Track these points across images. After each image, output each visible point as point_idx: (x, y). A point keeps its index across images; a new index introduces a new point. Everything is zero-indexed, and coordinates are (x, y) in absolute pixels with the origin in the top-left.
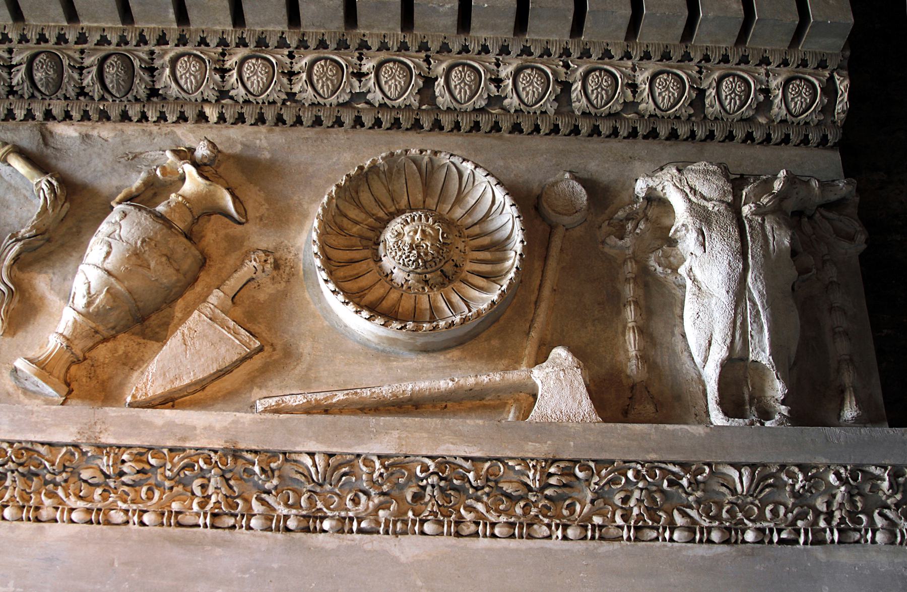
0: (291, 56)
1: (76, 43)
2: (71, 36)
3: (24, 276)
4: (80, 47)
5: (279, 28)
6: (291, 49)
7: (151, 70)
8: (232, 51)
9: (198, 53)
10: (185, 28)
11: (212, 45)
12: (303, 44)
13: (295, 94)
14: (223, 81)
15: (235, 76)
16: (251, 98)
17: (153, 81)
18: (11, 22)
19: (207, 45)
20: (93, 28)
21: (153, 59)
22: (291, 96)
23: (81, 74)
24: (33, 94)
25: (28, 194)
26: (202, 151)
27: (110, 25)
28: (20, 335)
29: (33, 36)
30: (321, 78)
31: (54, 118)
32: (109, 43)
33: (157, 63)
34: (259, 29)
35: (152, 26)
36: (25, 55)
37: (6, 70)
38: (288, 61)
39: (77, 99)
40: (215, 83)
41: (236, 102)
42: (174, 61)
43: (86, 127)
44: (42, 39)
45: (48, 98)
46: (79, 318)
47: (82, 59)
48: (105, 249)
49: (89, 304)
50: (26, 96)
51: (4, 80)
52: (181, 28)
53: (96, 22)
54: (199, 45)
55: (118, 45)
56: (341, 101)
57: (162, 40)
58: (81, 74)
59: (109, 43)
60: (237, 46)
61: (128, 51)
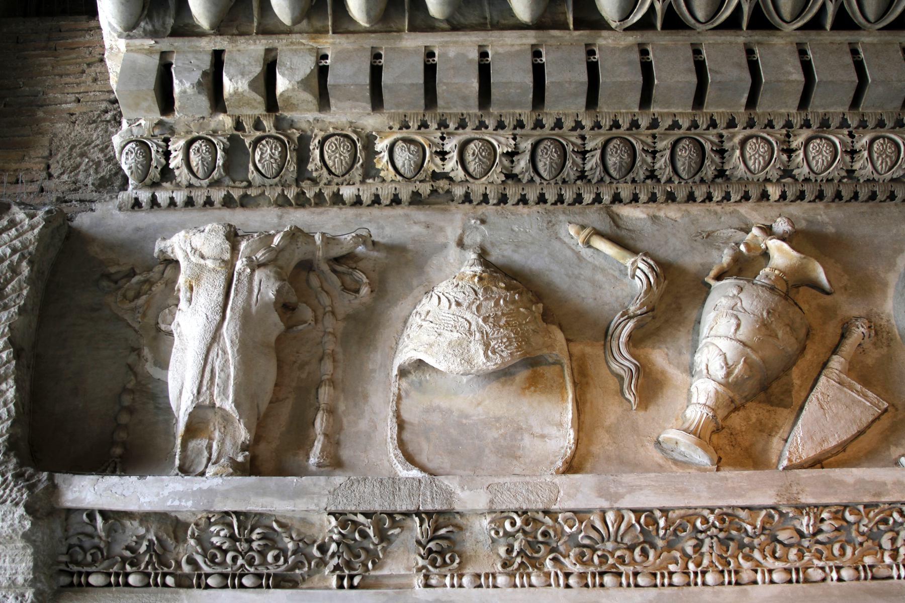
0: (851, 135)
1: (648, 128)
2: (644, 122)
3: (640, 352)
4: (650, 131)
5: (840, 110)
6: (850, 129)
7: (721, 152)
8: (796, 133)
9: (765, 135)
10: (752, 112)
11: (777, 127)
12: (863, 125)
13: (854, 171)
14: (789, 161)
15: (802, 155)
16: (812, 176)
17: (723, 163)
18: (584, 109)
19: (772, 127)
20: (664, 113)
21: (722, 142)
22: (850, 172)
23: (654, 158)
24: (602, 178)
25: (617, 274)
26: (781, 226)
27: (680, 110)
28: (652, 410)
29: (606, 122)
30: (881, 155)
31: (621, 201)
32: (680, 127)
33: (727, 145)
34: (821, 111)
35: (721, 110)
36: (599, 141)
37: (580, 156)
38: (849, 140)
39: (644, 182)
40: (782, 162)
41: (797, 180)
42: (743, 143)
43: (652, 208)
44: (616, 125)
45: (615, 182)
46: (720, 389)
47: (654, 143)
48: (734, 321)
49: (728, 374)
50: (594, 181)
51: (578, 166)
52: (749, 112)
53: (668, 108)
54: (765, 128)
55: (689, 129)
56: (895, 176)
57: (732, 124)
58: (654, 158)
59: (680, 127)
60: (801, 127)
61: (698, 135)
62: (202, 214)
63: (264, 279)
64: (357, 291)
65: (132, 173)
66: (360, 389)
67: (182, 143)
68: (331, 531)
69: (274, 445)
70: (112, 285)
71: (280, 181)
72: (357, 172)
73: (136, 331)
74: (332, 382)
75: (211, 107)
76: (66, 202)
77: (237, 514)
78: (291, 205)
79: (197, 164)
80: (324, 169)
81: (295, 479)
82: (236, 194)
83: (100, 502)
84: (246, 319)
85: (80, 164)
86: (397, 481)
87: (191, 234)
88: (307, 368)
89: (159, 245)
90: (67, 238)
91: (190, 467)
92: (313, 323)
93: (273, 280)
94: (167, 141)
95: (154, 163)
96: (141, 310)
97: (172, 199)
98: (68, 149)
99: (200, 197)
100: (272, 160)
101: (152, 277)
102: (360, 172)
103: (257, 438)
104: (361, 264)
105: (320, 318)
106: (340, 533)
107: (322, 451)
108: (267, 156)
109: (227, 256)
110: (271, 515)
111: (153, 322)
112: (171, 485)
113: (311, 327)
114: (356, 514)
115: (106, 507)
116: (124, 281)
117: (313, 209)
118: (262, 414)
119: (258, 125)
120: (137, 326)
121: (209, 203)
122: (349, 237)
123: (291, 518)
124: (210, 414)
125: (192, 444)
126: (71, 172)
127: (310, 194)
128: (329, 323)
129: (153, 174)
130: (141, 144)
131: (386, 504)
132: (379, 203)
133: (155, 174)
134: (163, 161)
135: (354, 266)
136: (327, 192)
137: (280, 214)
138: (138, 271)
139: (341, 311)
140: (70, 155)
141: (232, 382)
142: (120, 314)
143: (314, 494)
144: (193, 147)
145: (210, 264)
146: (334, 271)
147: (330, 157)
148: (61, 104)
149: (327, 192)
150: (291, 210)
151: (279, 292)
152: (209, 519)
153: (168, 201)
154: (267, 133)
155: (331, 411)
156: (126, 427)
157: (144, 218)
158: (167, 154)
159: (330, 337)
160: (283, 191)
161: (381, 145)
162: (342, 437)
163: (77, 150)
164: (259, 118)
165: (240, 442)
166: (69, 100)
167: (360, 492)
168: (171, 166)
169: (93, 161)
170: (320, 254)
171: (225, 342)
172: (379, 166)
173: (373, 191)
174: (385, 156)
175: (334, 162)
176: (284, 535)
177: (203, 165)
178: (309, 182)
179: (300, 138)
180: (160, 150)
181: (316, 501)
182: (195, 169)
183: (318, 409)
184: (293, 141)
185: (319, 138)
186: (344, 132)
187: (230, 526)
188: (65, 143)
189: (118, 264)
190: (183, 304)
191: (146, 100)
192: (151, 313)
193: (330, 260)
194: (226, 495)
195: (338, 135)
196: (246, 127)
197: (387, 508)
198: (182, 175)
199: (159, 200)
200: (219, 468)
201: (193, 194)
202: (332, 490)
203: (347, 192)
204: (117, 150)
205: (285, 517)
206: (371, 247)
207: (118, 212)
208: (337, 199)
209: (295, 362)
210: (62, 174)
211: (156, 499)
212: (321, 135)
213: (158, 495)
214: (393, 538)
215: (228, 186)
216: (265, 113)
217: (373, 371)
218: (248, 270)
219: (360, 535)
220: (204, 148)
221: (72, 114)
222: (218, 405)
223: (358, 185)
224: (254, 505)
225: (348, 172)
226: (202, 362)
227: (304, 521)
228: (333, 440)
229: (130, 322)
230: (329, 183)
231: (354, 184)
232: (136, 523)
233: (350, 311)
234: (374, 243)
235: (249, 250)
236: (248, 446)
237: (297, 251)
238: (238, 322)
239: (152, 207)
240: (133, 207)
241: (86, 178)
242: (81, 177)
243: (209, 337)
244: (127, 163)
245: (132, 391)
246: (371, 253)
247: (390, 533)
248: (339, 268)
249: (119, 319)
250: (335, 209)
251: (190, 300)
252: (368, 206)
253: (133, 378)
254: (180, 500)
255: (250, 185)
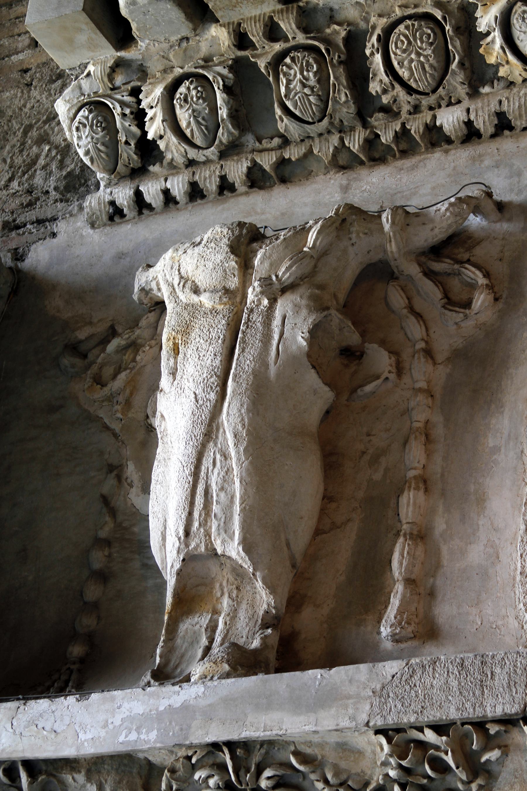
62: (220, 208)
63: (290, 314)
64: (467, 304)
65: (92, 160)
66: (472, 488)
67: (159, 91)
68: (385, 764)
69: (325, 610)
70: (78, 361)
71: (331, 123)
72: (456, 81)
73: (115, 435)
74: (424, 482)
75: (189, 17)
76: (18, 227)
77: (231, 745)
78: (362, 163)
79: (189, 124)
80: (398, 88)
81: (317, 673)
82: (267, 161)
83: (20, 747)
84: (260, 392)
85: (38, 156)
86: (489, 660)
87: (180, 252)
88: (383, 461)
89: (141, 279)
90: (15, 291)
91: (176, 667)
92: (392, 376)
93: (304, 312)
94: (136, 92)
95: (122, 137)
96: (121, 399)
97: (166, 192)
98: (20, 134)
99: (209, 180)
100: (307, 91)
101: (138, 337)
102: (460, 77)
103: (294, 601)
104: (479, 253)
105: (406, 365)
106: (400, 766)
107: (400, 612)
108: (296, 85)
109: (234, 283)
110: (288, 743)
111: (141, 416)
112: (126, 705)
113: (390, 385)
114: (420, 729)
115: (30, 755)
116: (95, 351)
117: (399, 163)
118: (299, 558)
119: (273, 32)
120: (116, 426)
121: (226, 187)
122: (443, 207)
123: (321, 745)
124: (214, 568)
125: (185, 626)
126: (24, 174)
127: (386, 138)
128: (420, 372)
129: (125, 155)
130: (97, 106)
131: (468, 705)
132: (511, 128)
133: (128, 154)
134: (135, 129)
135: (466, 256)
136: (416, 127)
137: (344, 182)
138: (119, 329)
139: (443, 346)
140: (23, 144)
141: (237, 508)
142: (91, 410)
143: (348, 697)
144: (178, 96)
145: (206, 300)
146: (429, 274)
147: (401, 64)
148: (9, 56)
149: (416, 127)
150: (363, 172)
151: (314, 334)
152: (189, 758)
153: (161, 196)
154: (292, 43)
155: (421, 536)
156: (95, 606)
157: (132, 233)
158: (139, 117)
159: (421, 398)
160: (342, 140)
161: (486, 19)
162: (439, 582)
163: (34, 133)
164: (271, 18)
165: (261, 613)
166: (20, 45)
167: (425, 688)
168: (150, 136)
169: (57, 147)
170: (393, 248)
171: (225, 439)
172: (492, 60)
173: (494, 106)
174: (497, 37)
175: (410, 69)
176: (313, 777)
177: (198, 123)
178: (381, 115)
179: (347, 40)
180: (127, 111)
181: (351, 711)
182: (188, 133)
183: (397, 535)
184: (336, 47)
185: (378, 31)
186: (421, 10)
187: (222, 767)
188: (15, 125)
189: (91, 323)
190: (165, 382)
191: (80, 30)
192: (137, 401)
193: (423, 253)
194: (208, 715)
195: (410, 17)
196: (254, 39)
197: (472, 713)
198: (171, 147)
199: (148, 198)
200: (207, 665)
201: (197, 178)
202: (379, 687)
203: (449, 119)
204: (65, 125)
205: (310, 744)
206: (495, 214)
207: (91, 231)
208: (435, 137)
209: (364, 453)
210: (11, 180)
211: (103, 733)
212: (383, 22)
213: (105, 726)
214: (495, 768)
215: (253, 151)
216: (280, 7)
217: (496, 450)
218: (266, 302)
219: (432, 768)
220: (194, 93)
221: (26, 71)
222: (219, 552)
223: (466, 103)
224: (255, 727)
225: (440, 83)
226: (191, 479)
227: (344, 748)
228: (423, 588)
229: (106, 420)
230: (416, 109)
231: (459, 102)
232: (81, 778)
233: (459, 343)
234: (501, 206)
235: (266, 264)
236: (277, 618)
237: (351, 249)
238: (245, 400)
239: (140, 213)
240: (111, 218)
241: (46, 180)
242: (38, 180)
243: (199, 431)
244: (83, 143)
245: (107, 543)
246: (498, 225)
247: (483, 759)
248: (437, 267)
249: (92, 419)
250: (437, 155)
251: (173, 373)
252: (493, 136)
253: (108, 519)
254: (138, 730)
255: (286, 142)
